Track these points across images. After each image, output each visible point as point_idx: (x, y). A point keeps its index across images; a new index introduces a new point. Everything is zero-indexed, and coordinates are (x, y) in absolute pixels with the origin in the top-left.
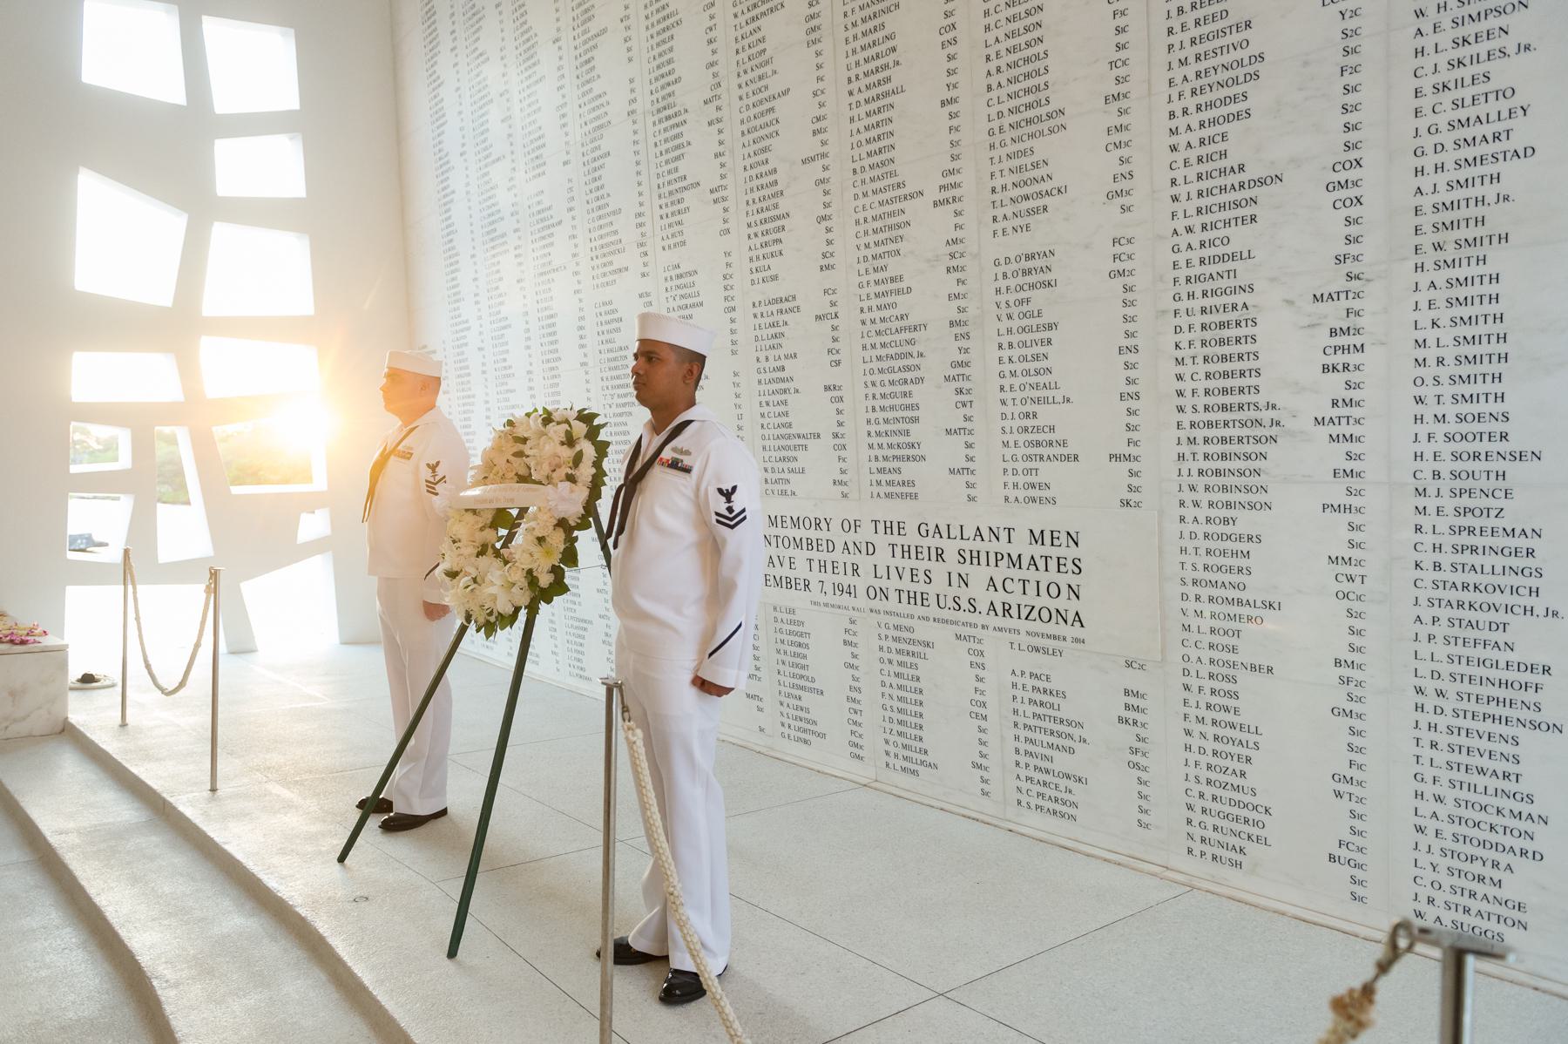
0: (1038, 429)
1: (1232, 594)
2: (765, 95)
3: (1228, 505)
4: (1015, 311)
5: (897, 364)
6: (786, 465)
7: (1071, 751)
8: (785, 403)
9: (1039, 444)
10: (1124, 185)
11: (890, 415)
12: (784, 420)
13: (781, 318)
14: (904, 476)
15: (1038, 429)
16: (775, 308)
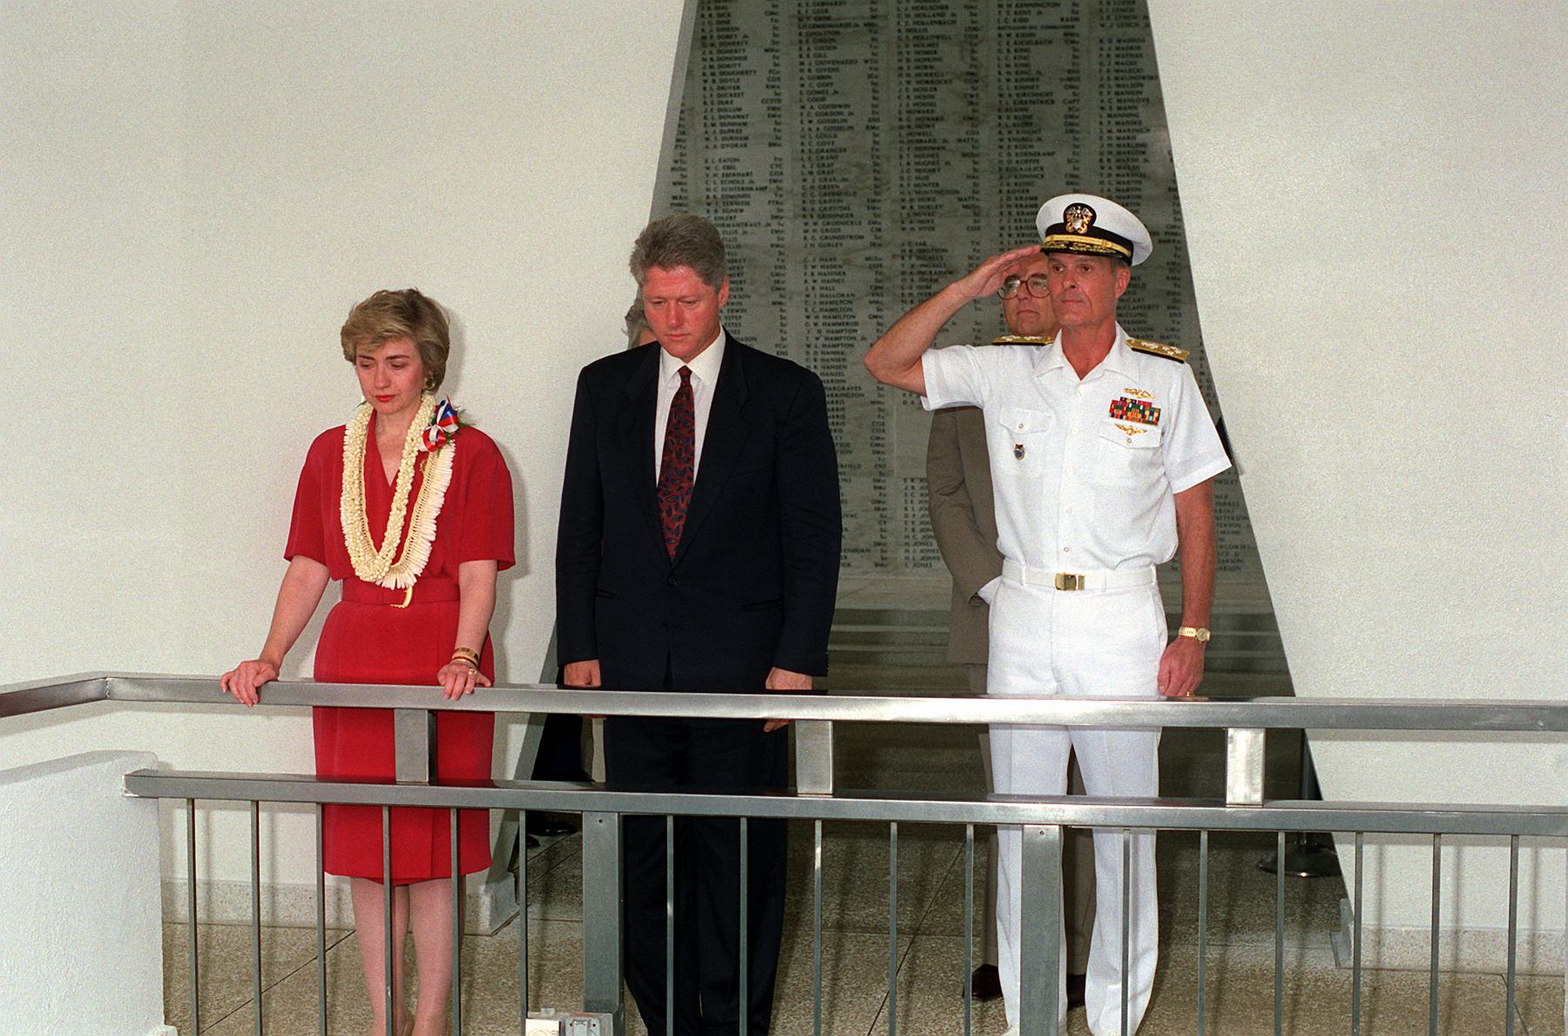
7: (1238, 533)
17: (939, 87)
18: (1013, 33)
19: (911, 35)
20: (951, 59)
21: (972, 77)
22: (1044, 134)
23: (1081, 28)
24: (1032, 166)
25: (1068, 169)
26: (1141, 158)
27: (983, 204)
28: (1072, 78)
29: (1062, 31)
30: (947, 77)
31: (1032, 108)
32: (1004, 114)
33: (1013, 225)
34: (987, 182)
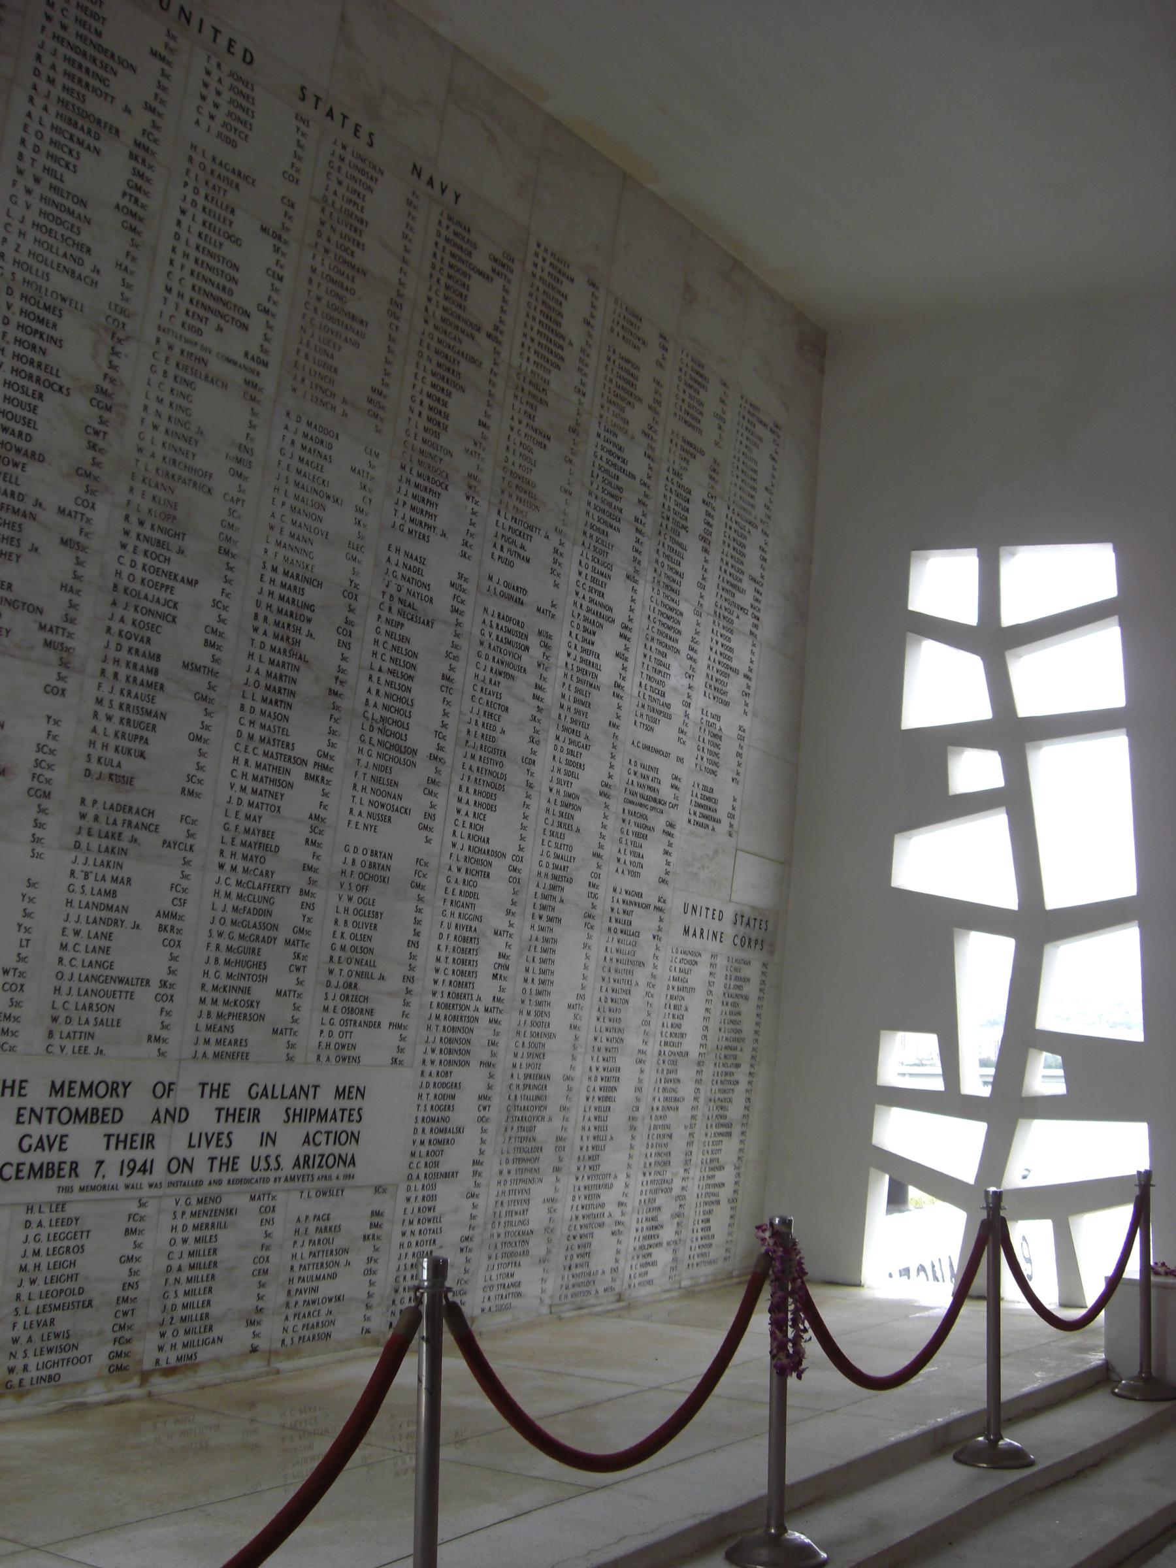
0: (356, 999)
1: (442, 1125)
2: (165, 567)
3: (450, 1063)
4: (356, 896)
5: (253, 919)
6: (91, 1015)
7: (333, 1276)
8: (108, 936)
9: (352, 1011)
10: (428, 822)
11: (236, 970)
12: (101, 957)
13: (127, 833)
14: (237, 1035)
15: (356, 999)
16: (120, 816)
17: (48, 393)
18: (179, 345)
19: (20, 274)
20: (76, 352)
21: (104, 397)
22: (189, 543)
23: (268, 380)
24: (163, 595)
25: (209, 616)
26: (305, 628)
27: (79, 646)
28: (242, 458)
29: (243, 374)
30: (64, 381)
31: (183, 491)
32: (139, 486)
33: (117, 699)
34: (93, 606)
